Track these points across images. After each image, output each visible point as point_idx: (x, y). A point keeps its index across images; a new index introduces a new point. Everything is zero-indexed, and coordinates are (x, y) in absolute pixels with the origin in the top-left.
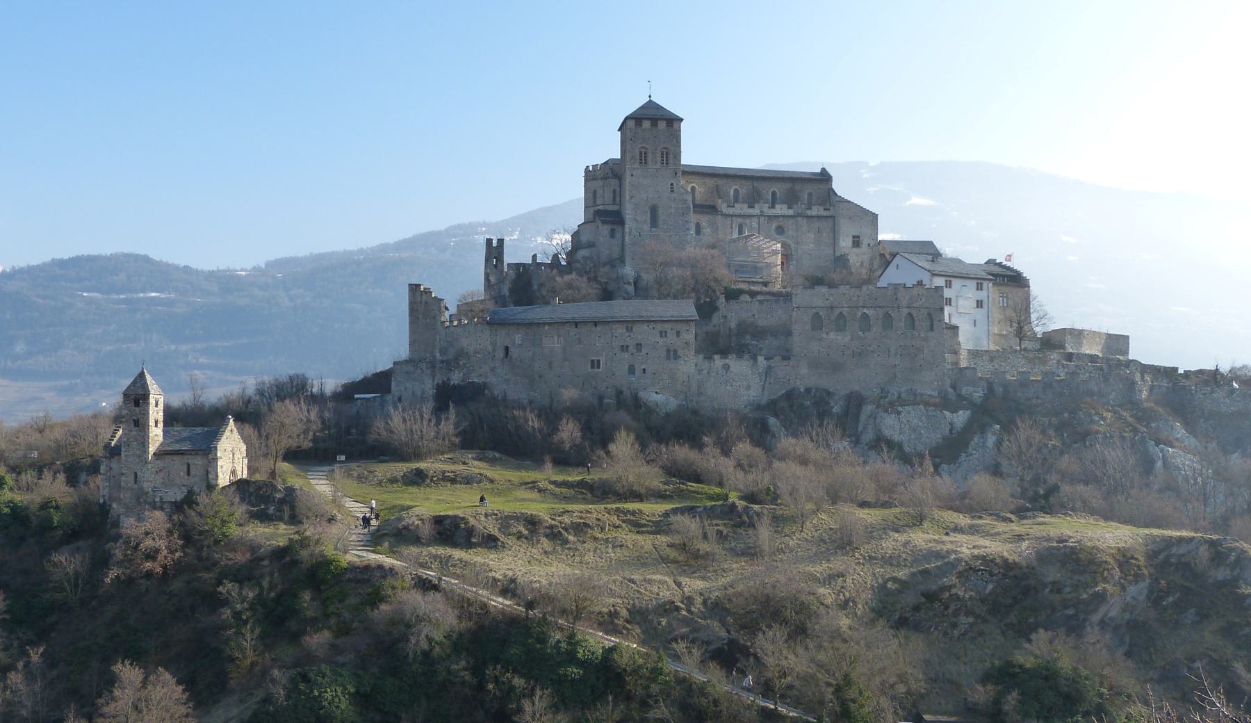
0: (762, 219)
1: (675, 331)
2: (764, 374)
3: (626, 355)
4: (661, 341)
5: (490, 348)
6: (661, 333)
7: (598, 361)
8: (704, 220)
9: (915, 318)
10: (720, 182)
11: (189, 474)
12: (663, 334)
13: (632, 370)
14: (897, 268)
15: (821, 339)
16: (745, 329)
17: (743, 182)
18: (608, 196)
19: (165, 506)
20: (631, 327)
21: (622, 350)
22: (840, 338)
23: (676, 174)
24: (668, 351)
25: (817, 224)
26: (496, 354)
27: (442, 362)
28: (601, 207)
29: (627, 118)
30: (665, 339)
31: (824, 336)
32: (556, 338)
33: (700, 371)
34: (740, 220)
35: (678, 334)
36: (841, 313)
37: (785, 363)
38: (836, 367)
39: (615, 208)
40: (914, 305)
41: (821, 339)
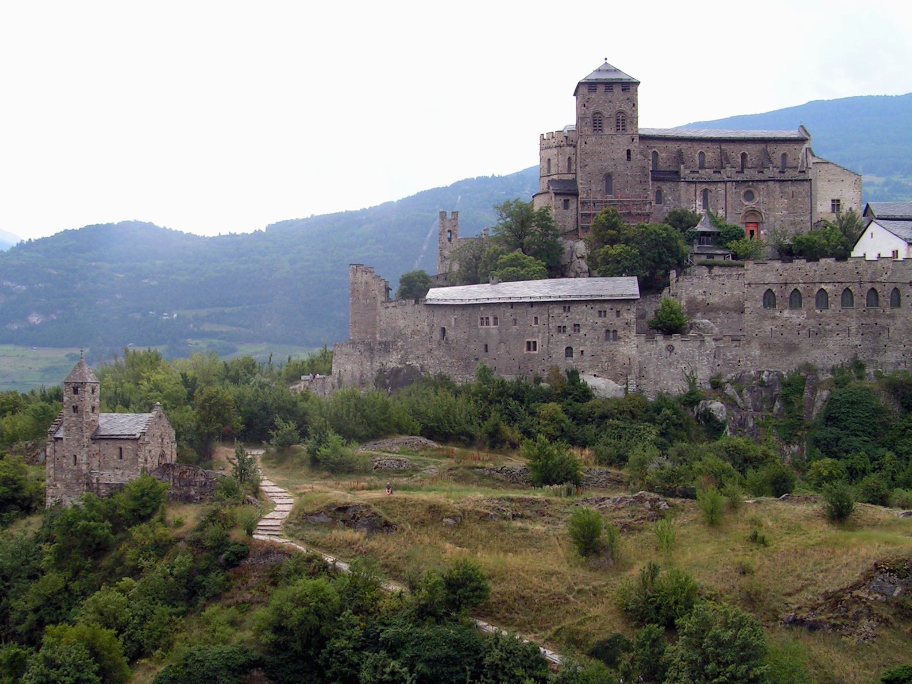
1: (614, 310)
2: (712, 356)
3: (563, 337)
4: (600, 321)
5: (427, 329)
6: (600, 312)
7: (535, 343)
8: (666, 187)
9: (880, 294)
10: (684, 146)
11: (121, 458)
13: (569, 351)
14: (872, 237)
15: (774, 318)
16: (694, 307)
17: (709, 144)
18: (563, 164)
19: (101, 487)
20: (569, 307)
21: (560, 332)
22: (794, 316)
23: (633, 140)
24: (608, 331)
25: (790, 188)
26: (434, 337)
27: (380, 343)
28: (555, 177)
29: (580, 84)
30: (604, 319)
31: (778, 314)
32: (491, 319)
33: (641, 353)
34: (704, 186)
35: (618, 313)
36: (796, 289)
37: (735, 343)
38: (791, 348)
40: (878, 280)
41: (774, 318)
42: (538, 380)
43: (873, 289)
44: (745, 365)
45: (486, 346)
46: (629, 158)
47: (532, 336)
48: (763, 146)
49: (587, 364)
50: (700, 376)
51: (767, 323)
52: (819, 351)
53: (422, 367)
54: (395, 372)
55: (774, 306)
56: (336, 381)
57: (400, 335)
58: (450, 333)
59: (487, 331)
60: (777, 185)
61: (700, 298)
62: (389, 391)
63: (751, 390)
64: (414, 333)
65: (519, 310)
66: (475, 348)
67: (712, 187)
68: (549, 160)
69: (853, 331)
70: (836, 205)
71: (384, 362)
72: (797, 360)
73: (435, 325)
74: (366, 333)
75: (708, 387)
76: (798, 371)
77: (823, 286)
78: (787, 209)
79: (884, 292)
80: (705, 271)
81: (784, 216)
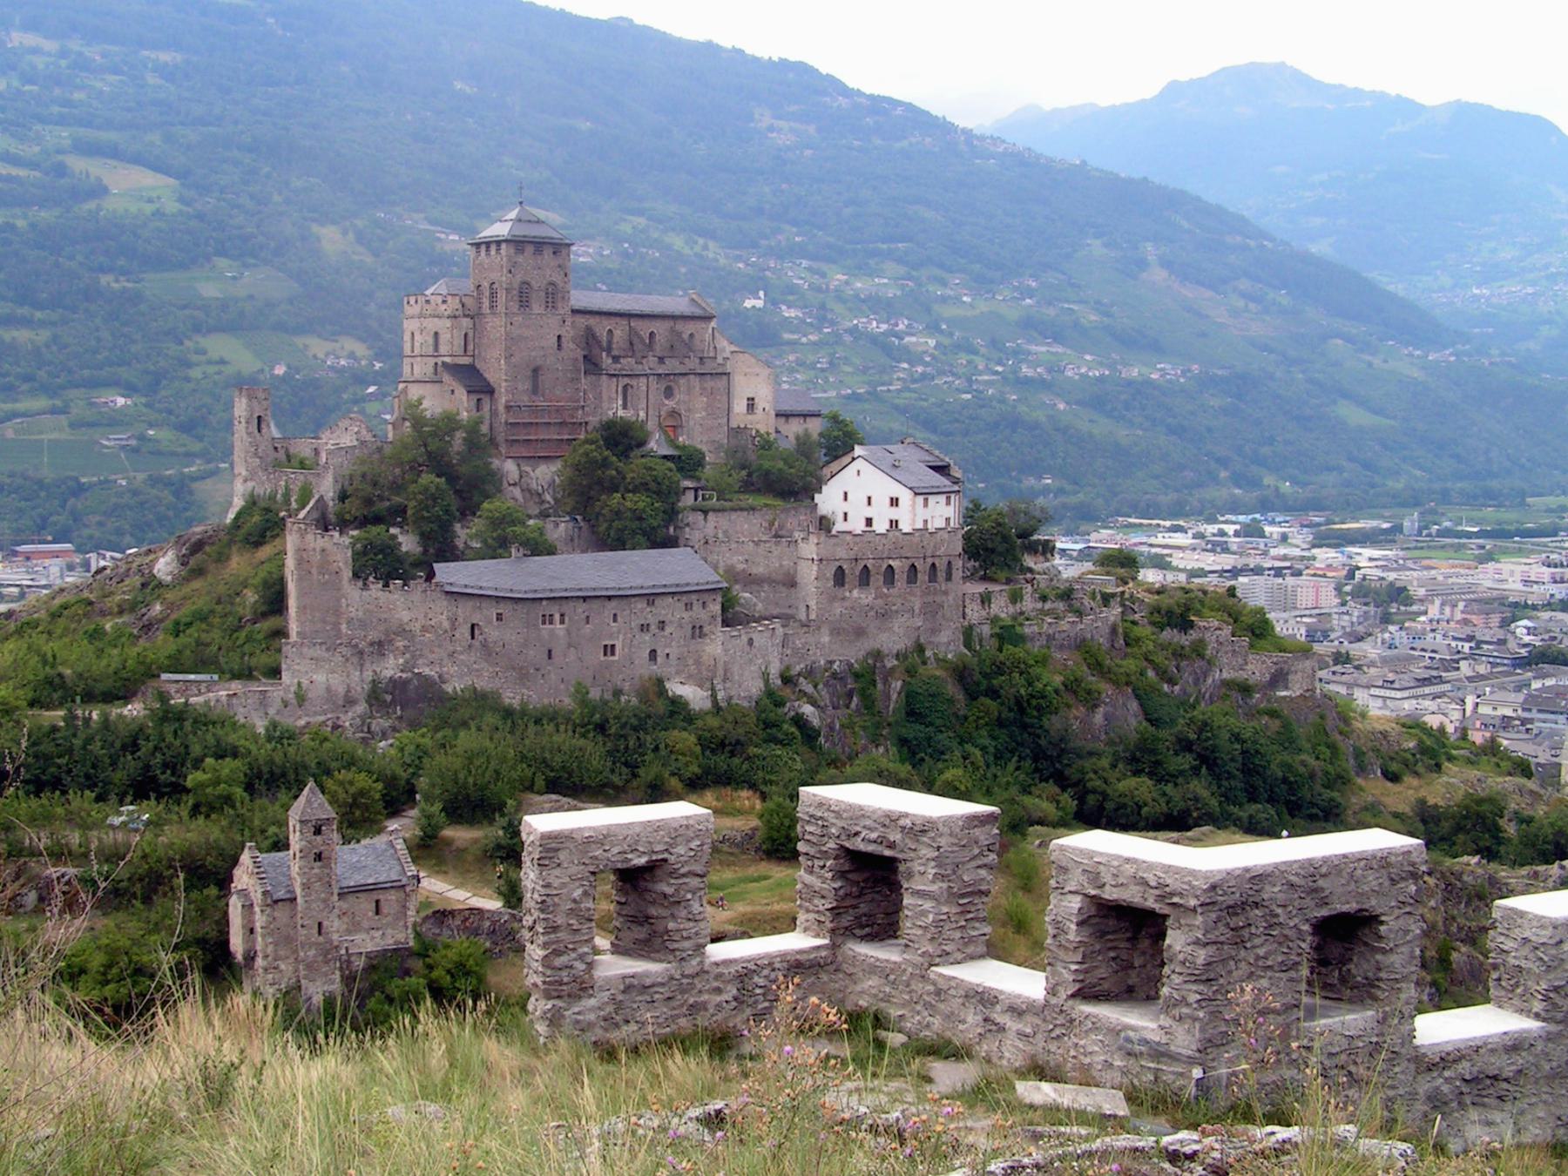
0: (651, 378)
3: (647, 637)
4: (686, 615)
5: (446, 625)
7: (613, 646)
10: (592, 321)
12: (688, 606)
15: (843, 599)
17: (618, 319)
18: (460, 342)
24: (694, 627)
25: (710, 383)
26: (457, 635)
28: (448, 360)
30: (690, 613)
31: (847, 594)
32: (557, 617)
33: (726, 651)
34: (626, 380)
37: (805, 629)
38: (860, 632)
39: (466, 361)
41: (843, 599)
42: (618, 693)
43: (933, 565)
44: (815, 654)
45: (550, 651)
46: (559, 346)
47: (611, 636)
48: (672, 323)
49: (673, 670)
50: (773, 671)
51: (836, 604)
52: (886, 635)
53: (440, 677)
54: (397, 685)
55: (843, 585)
56: (291, 696)
57: (403, 631)
58: (492, 633)
59: (552, 632)
60: (697, 379)
61: (740, 567)
62: (399, 713)
63: (826, 685)
64: (424, 629)
65: (596, 605)
66: (535, 654)
67: (634, 382)
68: (436, 334)
69: (917, 611)
70: (751, 404)
71: (378, 670)
72: (867, 645)
73: (461, 620)
74: (324, 621)
75: (779, 682)
76: (865, 659)
77: (891, 562)
78: (706, 410)
79: (941, 565)
80: (700, 517)
81: (703, 418)
